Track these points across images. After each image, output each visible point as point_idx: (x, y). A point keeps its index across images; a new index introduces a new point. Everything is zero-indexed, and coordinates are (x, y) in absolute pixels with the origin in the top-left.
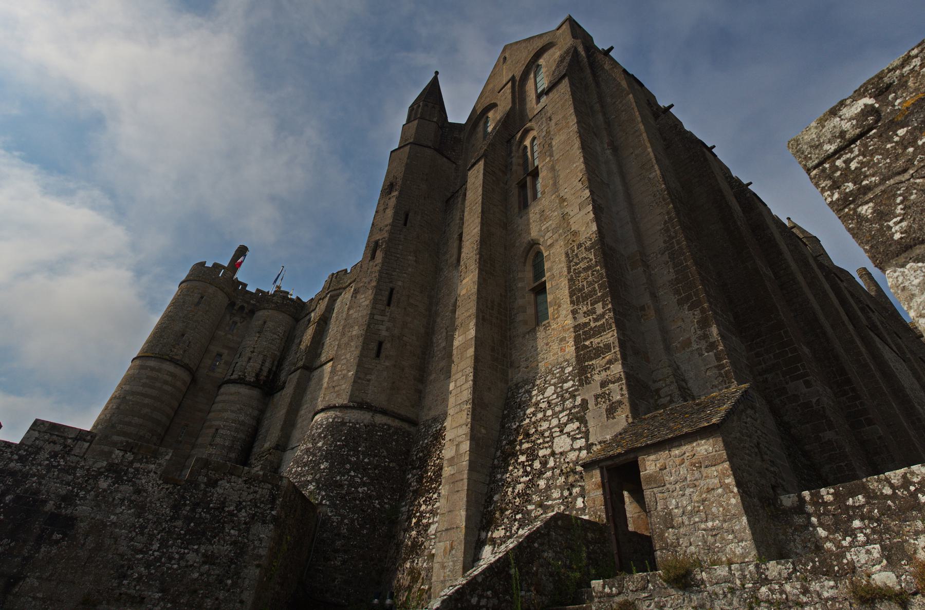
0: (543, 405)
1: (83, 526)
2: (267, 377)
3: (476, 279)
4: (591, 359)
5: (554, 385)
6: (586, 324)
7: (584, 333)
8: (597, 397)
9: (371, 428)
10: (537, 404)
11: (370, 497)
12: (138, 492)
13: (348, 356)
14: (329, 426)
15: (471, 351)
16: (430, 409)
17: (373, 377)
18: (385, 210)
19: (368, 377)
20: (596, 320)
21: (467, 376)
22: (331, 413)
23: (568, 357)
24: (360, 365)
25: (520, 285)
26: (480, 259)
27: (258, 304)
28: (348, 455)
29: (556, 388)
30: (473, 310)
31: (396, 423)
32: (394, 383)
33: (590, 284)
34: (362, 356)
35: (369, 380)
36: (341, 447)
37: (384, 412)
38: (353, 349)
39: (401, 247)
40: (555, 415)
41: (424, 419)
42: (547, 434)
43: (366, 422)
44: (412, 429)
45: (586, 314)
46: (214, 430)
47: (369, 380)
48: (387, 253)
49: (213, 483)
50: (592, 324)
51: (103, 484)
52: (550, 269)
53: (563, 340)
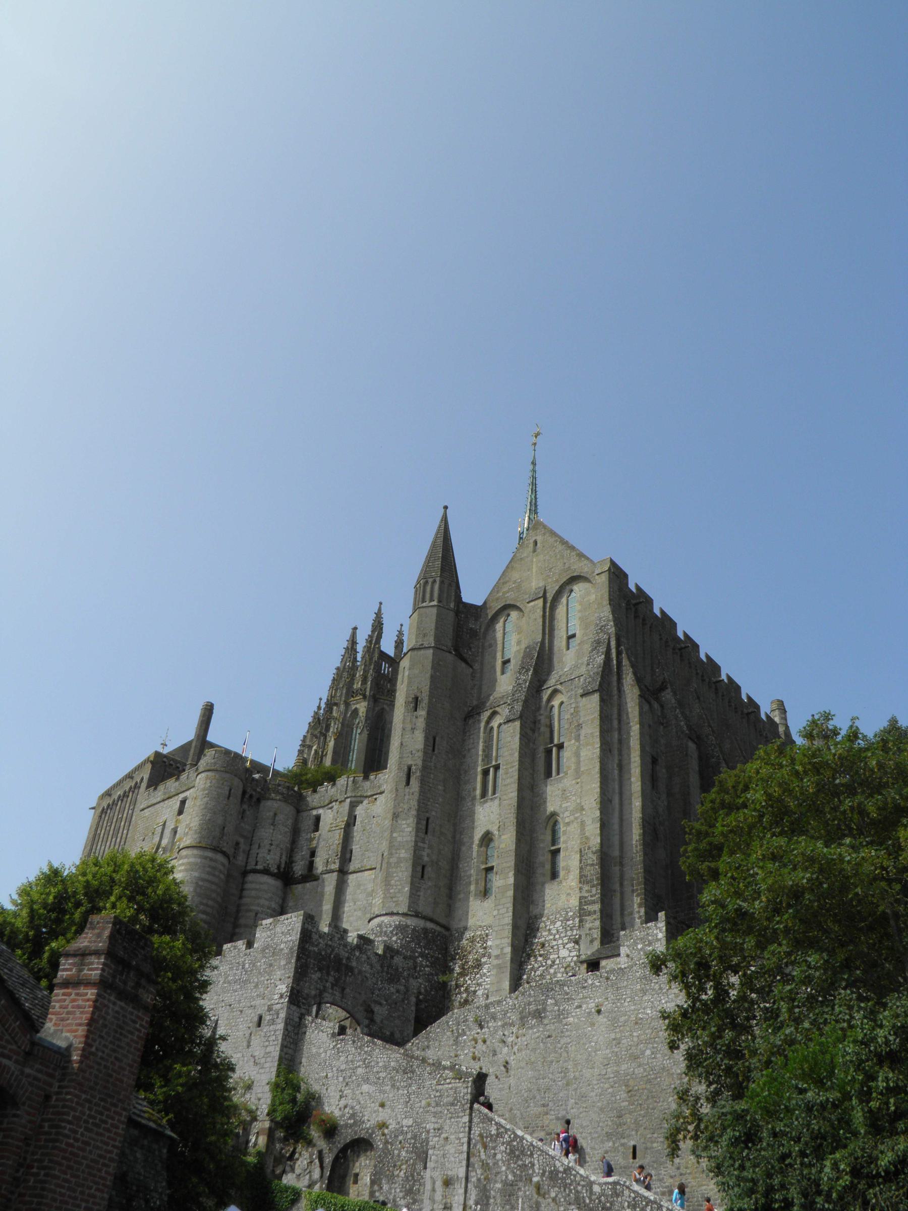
0: (554, 932)
1: (356, 971)
2: (285, 868)
3: (514, 839)
4: (586, 916)
5: (561, 921)
6: (586, 897)
7: (585, 902)
8: (586, 935)
9: (425, 931)
10: (549, 930)
11: (432, 974)
12: (368, 958)
13: (400, 874)
14: (396, 927)
15: (511, 893)
16: (460, 920)
17: (422, 894)
18: (413, 729)
19: (418, 893)
20: (591, 896)
21: (508, 908)
22: (395, 918)
23: (570, 906)
24: (412, 884)
25: (542, 845)
26: (517, 822)
27: (262, 792)
28: (415, 947)
29: (562, 923)
30: (513, 863)
31: (438, 928)
32: (435, 899)
33: (592, 875)
34: (413, 876)
35: (419, 896)
36: (410, 942)
37: (432, 920)
38: (403, 869)
39: (432, 776)
40: (561, 938)
41: (455, 926)
42: (555, 947)
43: (422, 926)
44: (447, 933)
45: (587, 891)
46: (254, 914)
47: (419, 896)
48: (423, 782)
49: (392, 957)
50: (590, 898)
51: (357, 954)
52: (565, 842)
53: (569, 894)
